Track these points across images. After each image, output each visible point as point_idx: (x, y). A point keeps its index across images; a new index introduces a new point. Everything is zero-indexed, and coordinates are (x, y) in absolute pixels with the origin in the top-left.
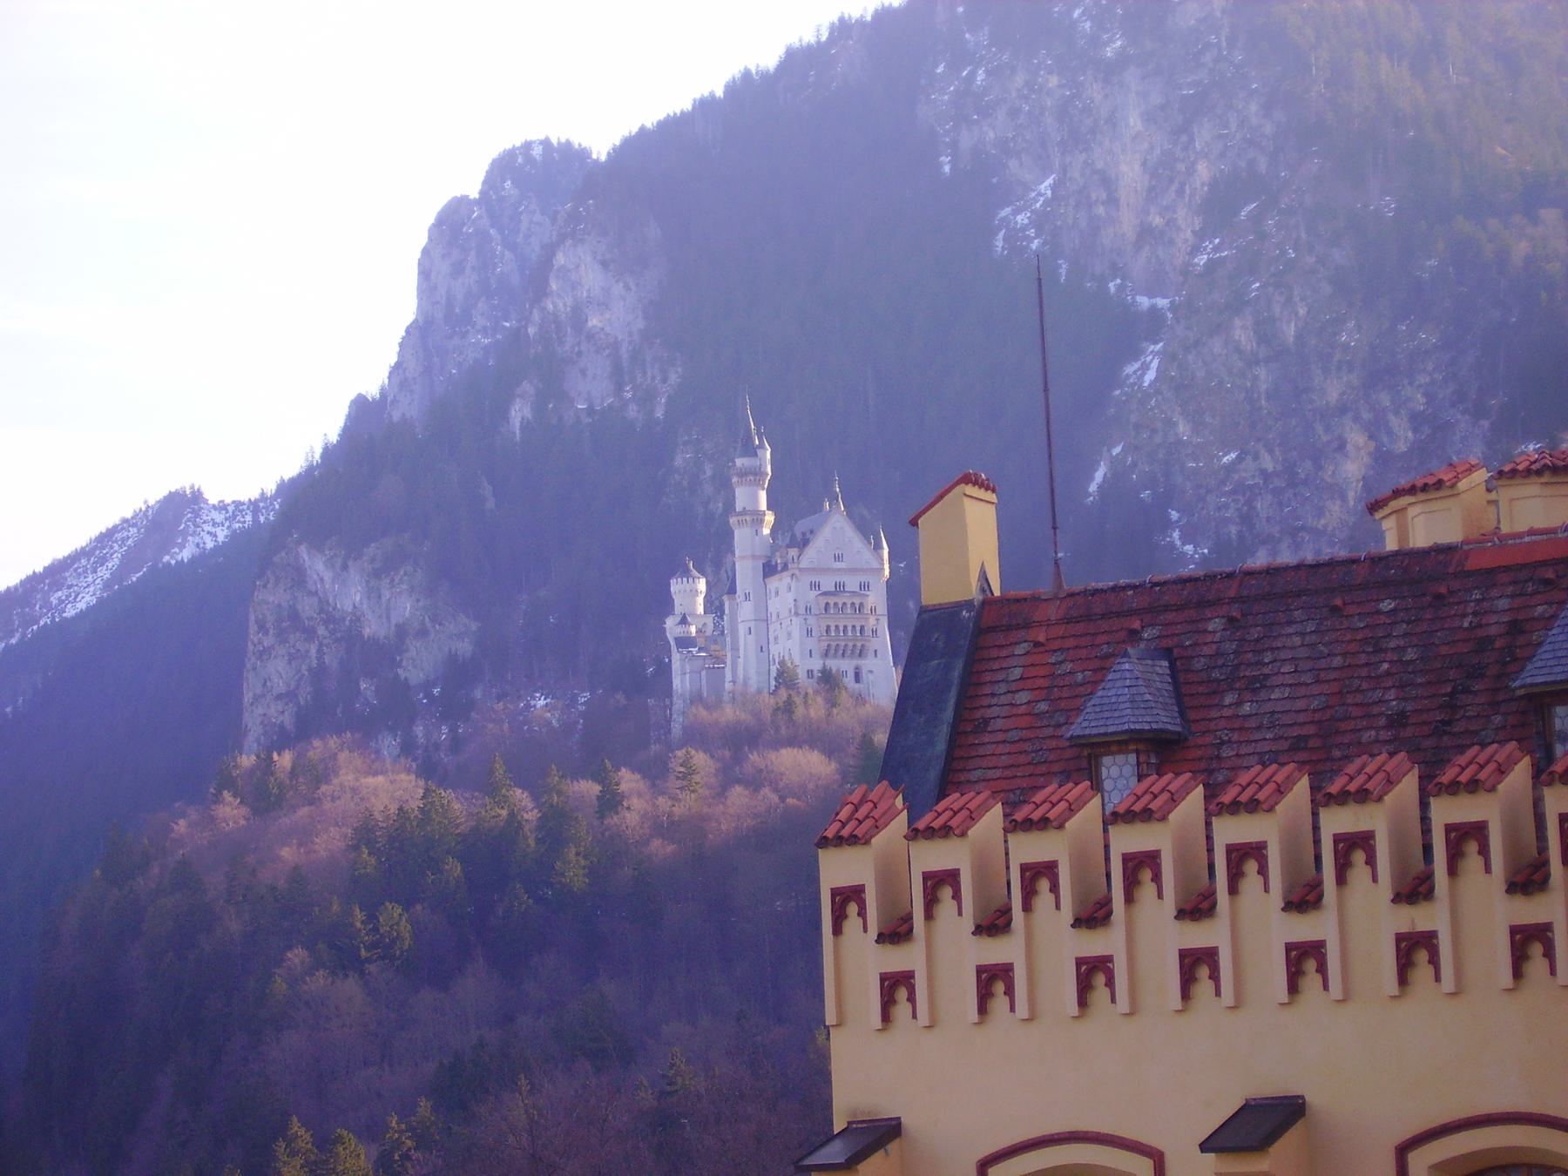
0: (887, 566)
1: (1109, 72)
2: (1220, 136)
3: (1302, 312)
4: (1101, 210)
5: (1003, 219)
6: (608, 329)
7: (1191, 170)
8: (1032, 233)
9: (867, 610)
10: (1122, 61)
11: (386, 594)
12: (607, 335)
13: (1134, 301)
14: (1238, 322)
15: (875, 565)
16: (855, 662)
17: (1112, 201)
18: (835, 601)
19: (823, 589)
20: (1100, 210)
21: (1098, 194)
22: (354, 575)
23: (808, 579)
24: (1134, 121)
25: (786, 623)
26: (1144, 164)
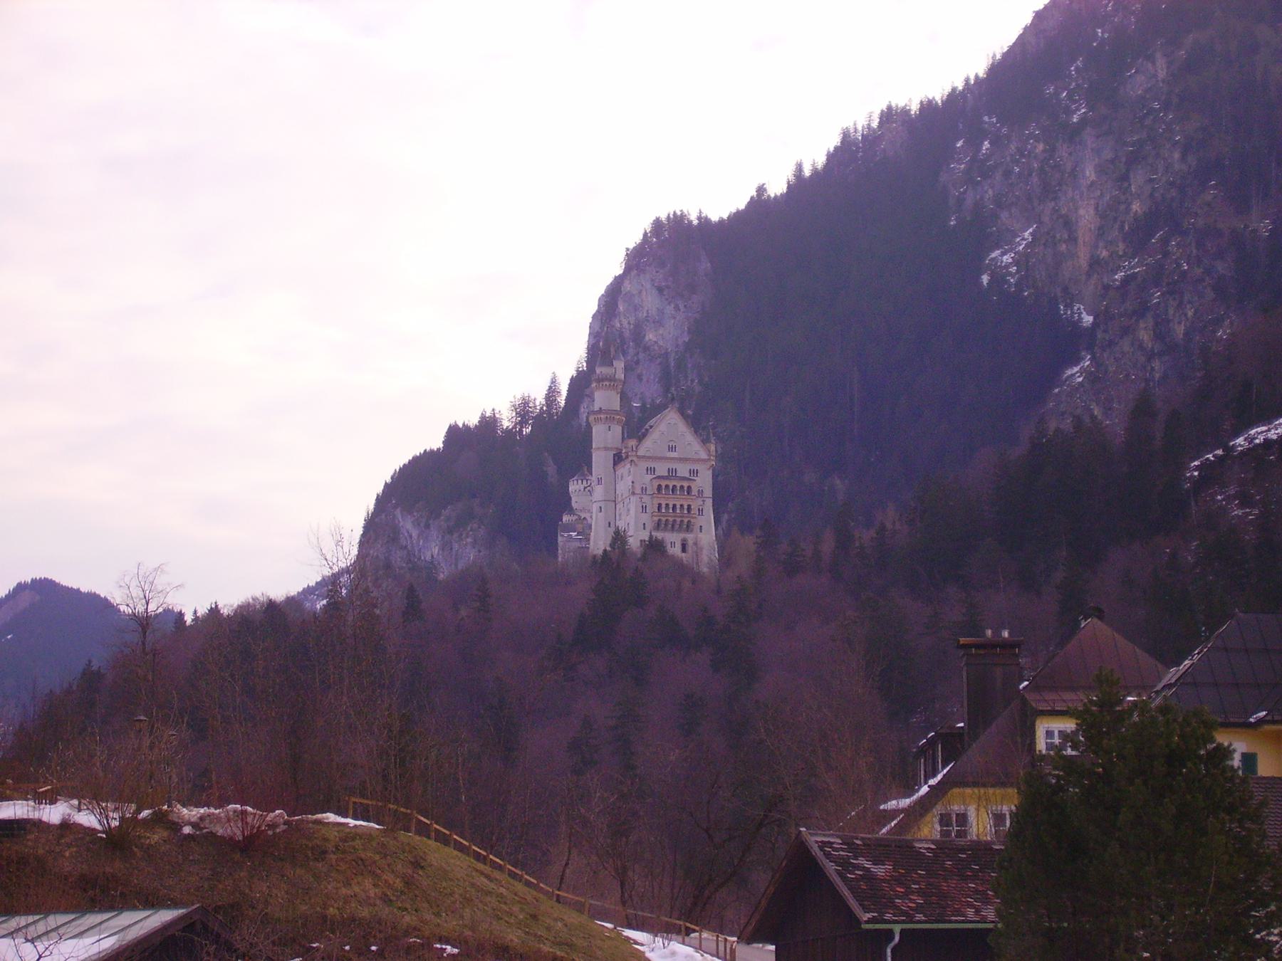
1: (1073, 134)
2: (1151, 180)
3: (1190, 314)
5: (993, 259)
6: (661, 343)
9: (694, 492)
10: (1084, 121)
11: (456, 546)
12: (660, 347)
14: (1142, 325)
16: (682, 535)
17: (1073, 239)
18: (668, 486)
19: (657, 473)
22: (434, 533)
23: (644, 465)
24: (1090, 173)
25: (627, 501)
26: (1096, 209)
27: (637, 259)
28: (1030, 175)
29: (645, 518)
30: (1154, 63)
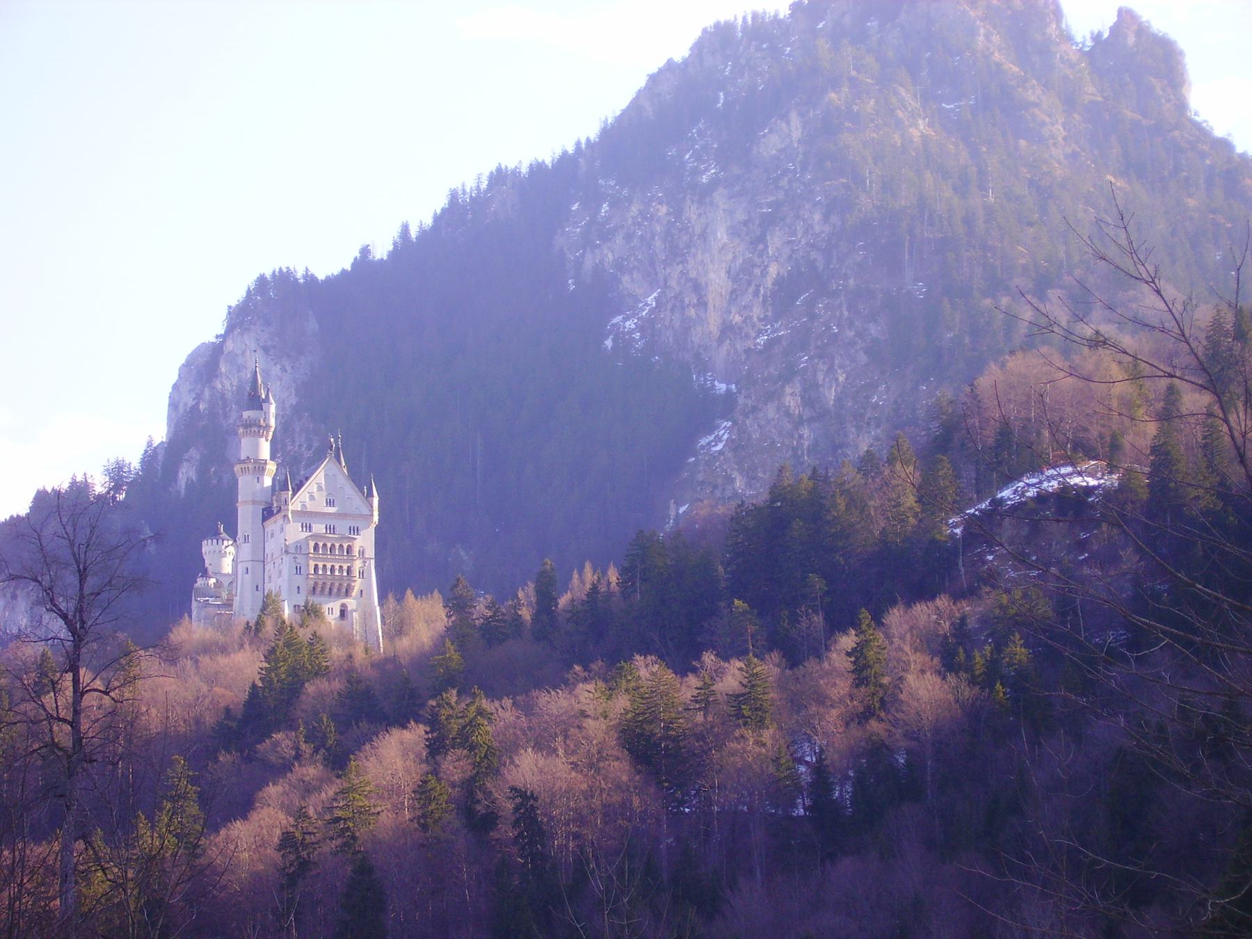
0: (376, 514)
1: (704, 195)
2: (789, 242)
4: (692, 312)
5: (613, 325)
7: (764, 273)
8: (637, 335)
10: (715, 183)
13: (714, 386)
14: (788, 390)
15: (366, 512)
17: (702, 304)
20: (692, 312)
21: (691, 298)
24: (721, 235)
25: (278, 561)
26: (728, 272)
27: (240, 318)
28: (653, 237)
29: (299, 580)
30: (788, 123)
